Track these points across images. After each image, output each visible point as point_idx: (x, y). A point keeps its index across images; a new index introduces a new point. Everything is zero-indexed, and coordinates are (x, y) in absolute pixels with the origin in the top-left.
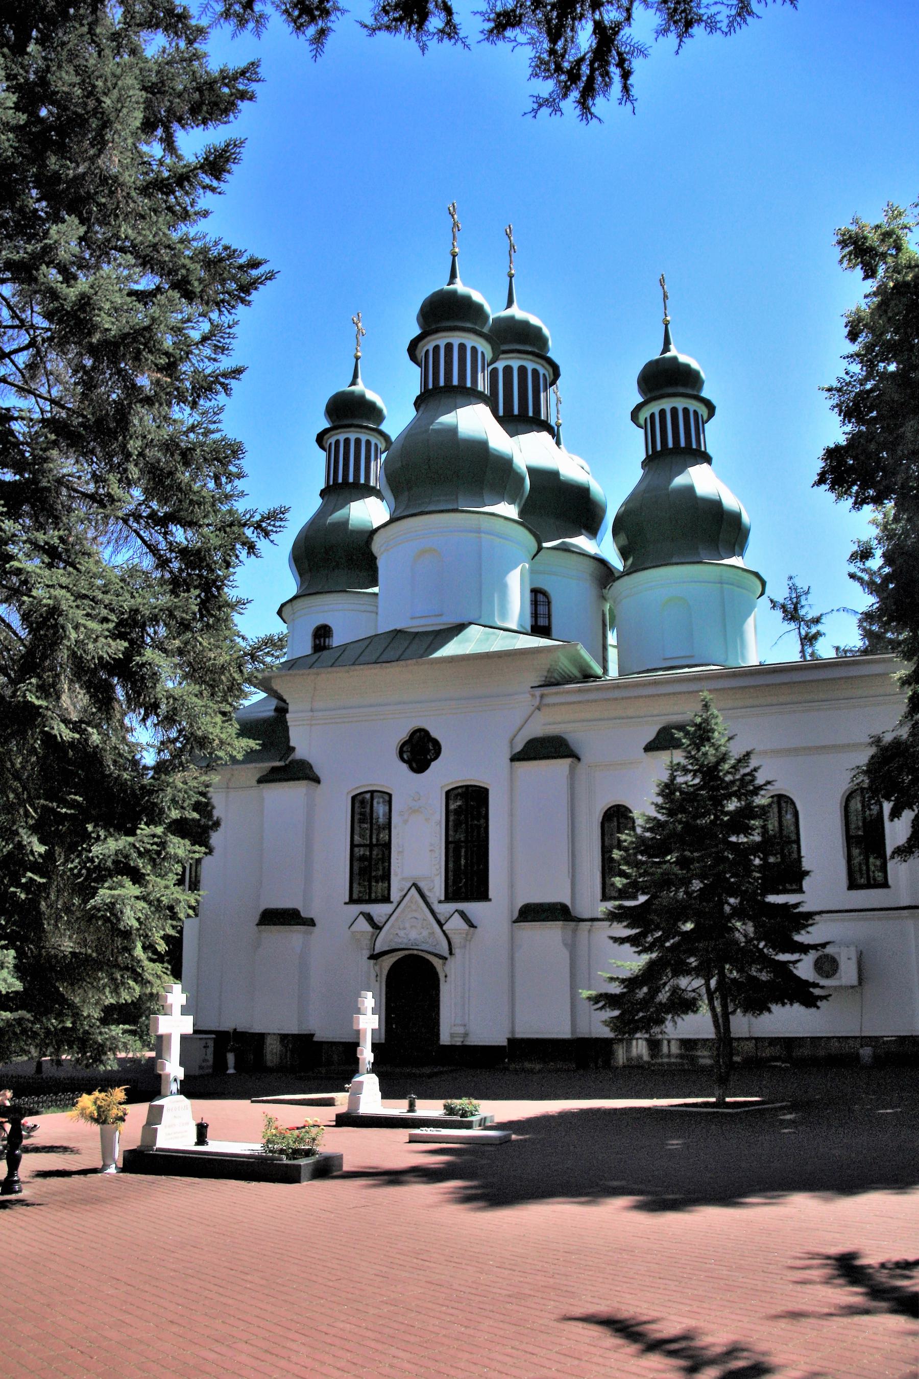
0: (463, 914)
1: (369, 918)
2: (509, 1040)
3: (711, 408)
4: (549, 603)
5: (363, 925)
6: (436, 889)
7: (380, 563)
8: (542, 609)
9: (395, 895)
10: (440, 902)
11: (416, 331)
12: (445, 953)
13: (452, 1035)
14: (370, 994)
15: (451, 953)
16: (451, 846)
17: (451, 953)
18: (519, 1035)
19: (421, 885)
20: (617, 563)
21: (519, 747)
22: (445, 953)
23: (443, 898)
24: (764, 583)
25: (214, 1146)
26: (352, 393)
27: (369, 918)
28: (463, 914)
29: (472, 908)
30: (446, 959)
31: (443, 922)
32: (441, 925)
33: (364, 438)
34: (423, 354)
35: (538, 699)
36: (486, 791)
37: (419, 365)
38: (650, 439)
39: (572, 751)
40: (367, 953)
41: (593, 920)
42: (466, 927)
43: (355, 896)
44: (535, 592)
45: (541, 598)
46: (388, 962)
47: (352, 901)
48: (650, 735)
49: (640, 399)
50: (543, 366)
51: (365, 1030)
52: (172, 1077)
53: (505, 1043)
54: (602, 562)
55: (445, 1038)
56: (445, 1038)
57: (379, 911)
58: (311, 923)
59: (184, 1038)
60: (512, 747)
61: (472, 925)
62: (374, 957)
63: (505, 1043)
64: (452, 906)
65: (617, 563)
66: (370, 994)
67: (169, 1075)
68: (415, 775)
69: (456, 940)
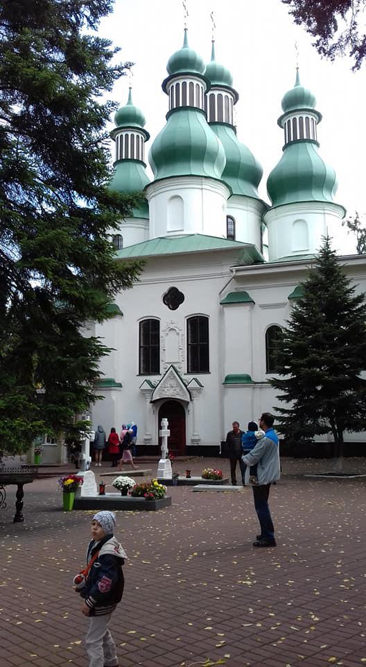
0: (196, 379)
1: (149, 382)
2: (222, 443)
3: (319, 116)
4: (234, 223)
5: (147, 386)
6: (183, 367)
7: (150, 204)
8: (231, 227)
9: (162, 371)
10: (185, 374)
11: (166, 75)
12: (189, 400)
13: (192, 440)
14: (166, 419)
16: (189, 346)
19: (175, 365)
22: (189, 400)
23: (186, 372)
24: (345, 211)
26: (129, 108)
27: (149, 382)
28: (196, 379)
29: (200, 377)
30: (188, 403)
32: (186, 386)
33: (135, 134)
36: (208, 319)
37: (168, 94)
39: (250, 298)
40: (149, 400)
42: (198, 386)
43: (142, 372)
44: (228, 217)
45: (229, 220)
46: (160, 404)
47: (140, 374)
49: (283, 113)
50: (230, 93)
51: (164, 437)
52: (86, 462)
54: (261, 201)
55: (188, 443)
56: (188, 443)
57: (154, 379)
58: (120, 385)
59: (168, 437)
62: (151, 402)
64: (191, 377)
66: (166, 419)
67: (84, 460)
68: (171, 311)
69: (194, 393)
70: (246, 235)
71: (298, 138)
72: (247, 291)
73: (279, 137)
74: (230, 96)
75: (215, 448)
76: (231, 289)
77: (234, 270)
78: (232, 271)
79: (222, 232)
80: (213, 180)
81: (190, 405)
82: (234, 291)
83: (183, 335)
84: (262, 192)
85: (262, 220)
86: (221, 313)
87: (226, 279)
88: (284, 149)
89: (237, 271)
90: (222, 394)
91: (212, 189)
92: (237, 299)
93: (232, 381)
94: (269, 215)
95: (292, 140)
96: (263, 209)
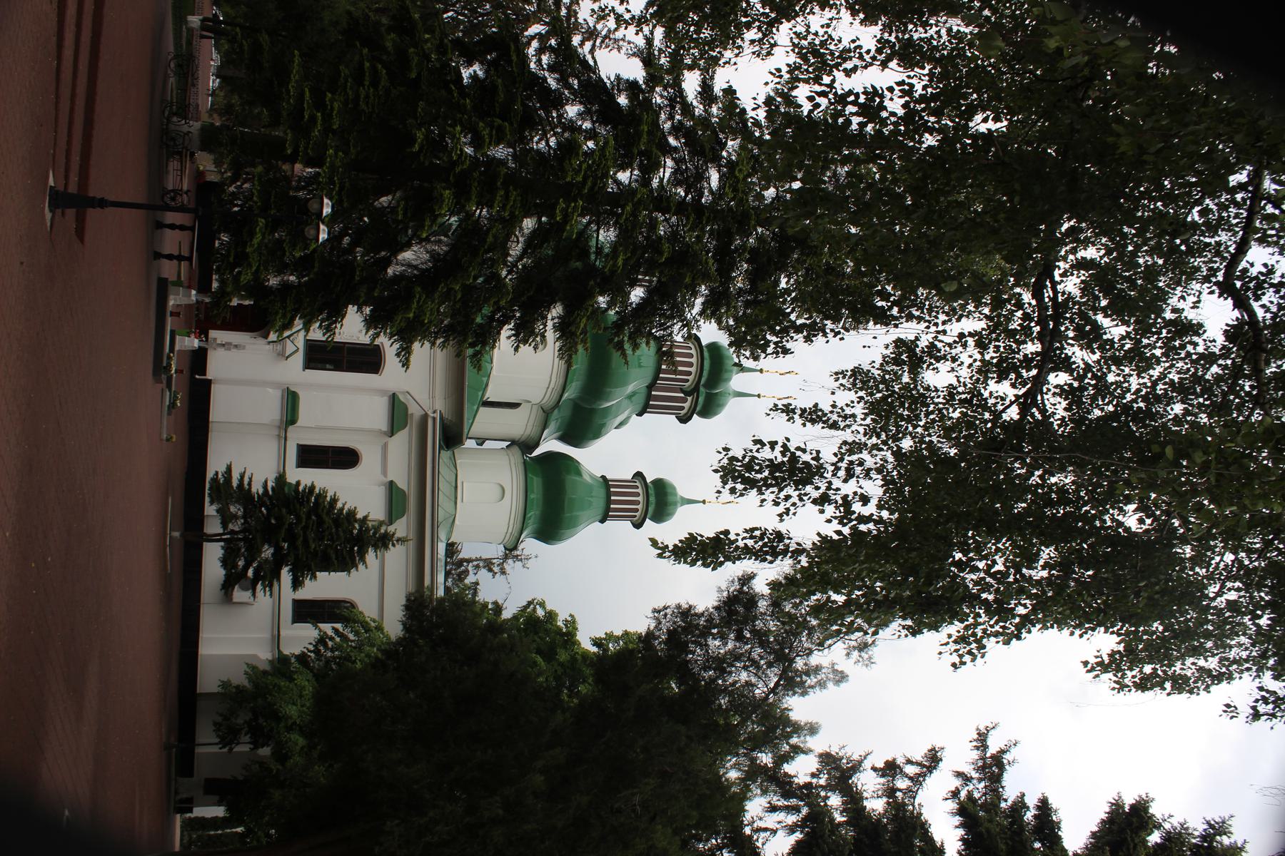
2: (209, 382)
15: (269, 343)
17: (269, 343)
18: (215, 389)
20: (537, 452)
21: (402, 398)
25: (169, 320)
29: (299, 358)
31: (291, 338)
34: (690, 345)
35: (432, 415)
38: (621, 483)
39: (397, 432)
41: (286, 439)
48: (402, 484)
53: (209, 376)
54: (537, 445)
60: (403, 393)
61: (287, 358)
63: (209, 376)
65: (537, 452)
69: (279, 347)
70: (485, 421)
71: (612, 498)
72: (407, 428)
73: (622, 472)
74: (683, 412)
75: (203, 371)
76: (414, 411)
77: (435, 415)
78: (434, 412)
79: (491, 395)
80: (560, 392)
81: (261, 341)
82: (409, 412)
83: (358, 338)
84: (550, 445)
85: (513, 443)
86: (382, 392)
87: (426, 404)
88: (603, 477)
89: (434, 419)
90: (274, 385)
91: (550, 390)
92: (397, 413)
93: (291, 401)
94: (516, 455)
95: (612, 490)
96: (526, 446)
